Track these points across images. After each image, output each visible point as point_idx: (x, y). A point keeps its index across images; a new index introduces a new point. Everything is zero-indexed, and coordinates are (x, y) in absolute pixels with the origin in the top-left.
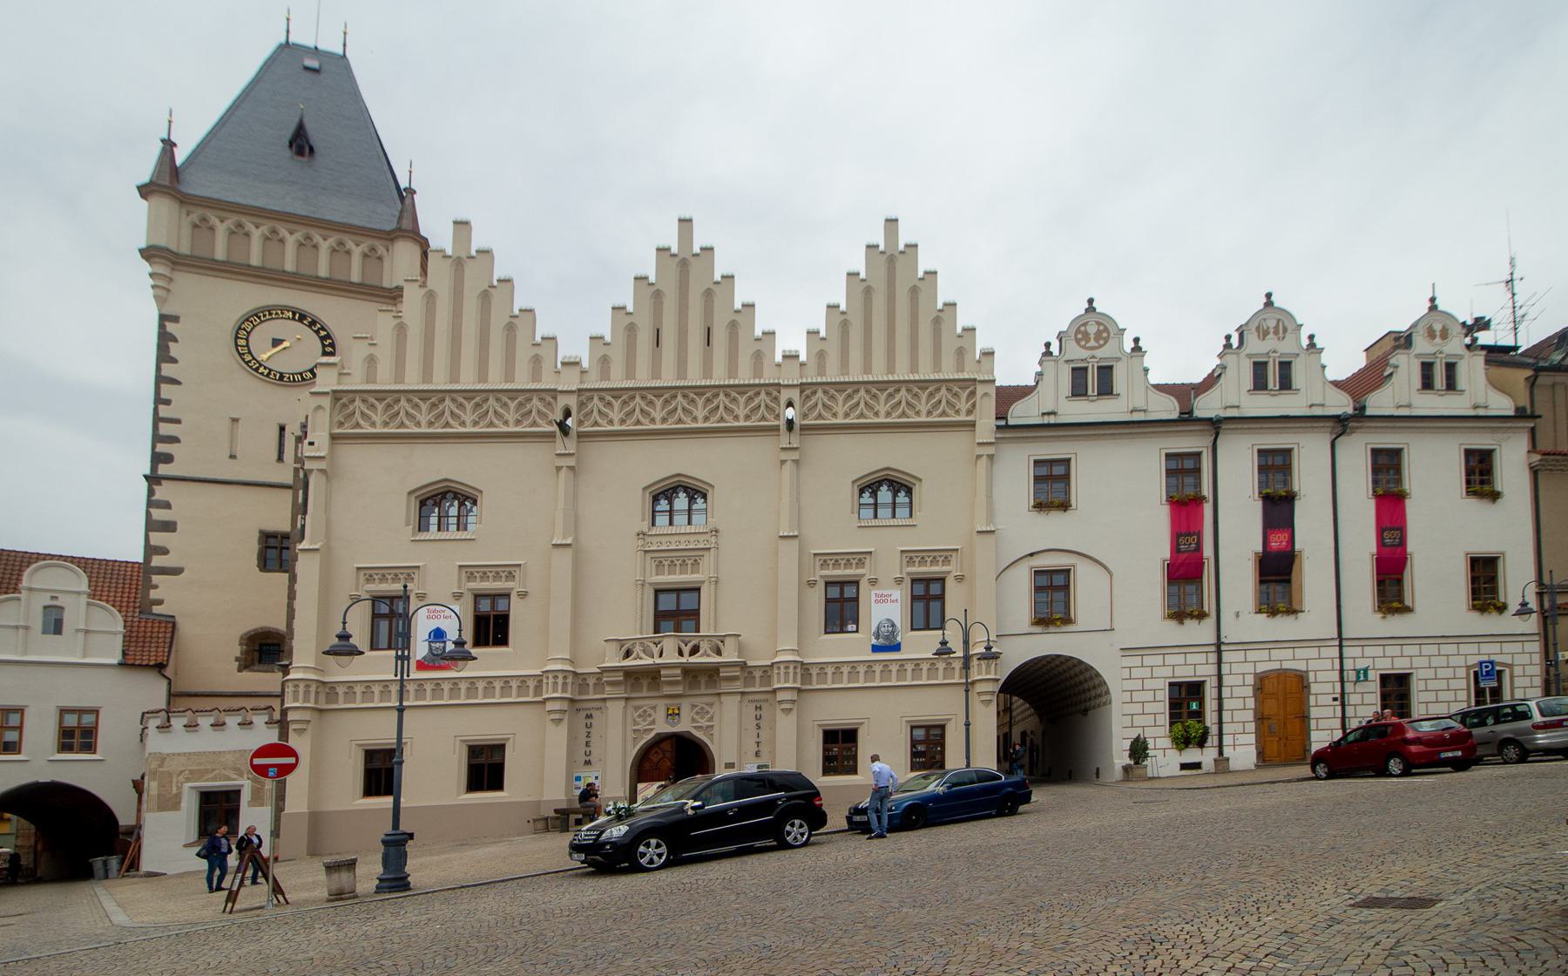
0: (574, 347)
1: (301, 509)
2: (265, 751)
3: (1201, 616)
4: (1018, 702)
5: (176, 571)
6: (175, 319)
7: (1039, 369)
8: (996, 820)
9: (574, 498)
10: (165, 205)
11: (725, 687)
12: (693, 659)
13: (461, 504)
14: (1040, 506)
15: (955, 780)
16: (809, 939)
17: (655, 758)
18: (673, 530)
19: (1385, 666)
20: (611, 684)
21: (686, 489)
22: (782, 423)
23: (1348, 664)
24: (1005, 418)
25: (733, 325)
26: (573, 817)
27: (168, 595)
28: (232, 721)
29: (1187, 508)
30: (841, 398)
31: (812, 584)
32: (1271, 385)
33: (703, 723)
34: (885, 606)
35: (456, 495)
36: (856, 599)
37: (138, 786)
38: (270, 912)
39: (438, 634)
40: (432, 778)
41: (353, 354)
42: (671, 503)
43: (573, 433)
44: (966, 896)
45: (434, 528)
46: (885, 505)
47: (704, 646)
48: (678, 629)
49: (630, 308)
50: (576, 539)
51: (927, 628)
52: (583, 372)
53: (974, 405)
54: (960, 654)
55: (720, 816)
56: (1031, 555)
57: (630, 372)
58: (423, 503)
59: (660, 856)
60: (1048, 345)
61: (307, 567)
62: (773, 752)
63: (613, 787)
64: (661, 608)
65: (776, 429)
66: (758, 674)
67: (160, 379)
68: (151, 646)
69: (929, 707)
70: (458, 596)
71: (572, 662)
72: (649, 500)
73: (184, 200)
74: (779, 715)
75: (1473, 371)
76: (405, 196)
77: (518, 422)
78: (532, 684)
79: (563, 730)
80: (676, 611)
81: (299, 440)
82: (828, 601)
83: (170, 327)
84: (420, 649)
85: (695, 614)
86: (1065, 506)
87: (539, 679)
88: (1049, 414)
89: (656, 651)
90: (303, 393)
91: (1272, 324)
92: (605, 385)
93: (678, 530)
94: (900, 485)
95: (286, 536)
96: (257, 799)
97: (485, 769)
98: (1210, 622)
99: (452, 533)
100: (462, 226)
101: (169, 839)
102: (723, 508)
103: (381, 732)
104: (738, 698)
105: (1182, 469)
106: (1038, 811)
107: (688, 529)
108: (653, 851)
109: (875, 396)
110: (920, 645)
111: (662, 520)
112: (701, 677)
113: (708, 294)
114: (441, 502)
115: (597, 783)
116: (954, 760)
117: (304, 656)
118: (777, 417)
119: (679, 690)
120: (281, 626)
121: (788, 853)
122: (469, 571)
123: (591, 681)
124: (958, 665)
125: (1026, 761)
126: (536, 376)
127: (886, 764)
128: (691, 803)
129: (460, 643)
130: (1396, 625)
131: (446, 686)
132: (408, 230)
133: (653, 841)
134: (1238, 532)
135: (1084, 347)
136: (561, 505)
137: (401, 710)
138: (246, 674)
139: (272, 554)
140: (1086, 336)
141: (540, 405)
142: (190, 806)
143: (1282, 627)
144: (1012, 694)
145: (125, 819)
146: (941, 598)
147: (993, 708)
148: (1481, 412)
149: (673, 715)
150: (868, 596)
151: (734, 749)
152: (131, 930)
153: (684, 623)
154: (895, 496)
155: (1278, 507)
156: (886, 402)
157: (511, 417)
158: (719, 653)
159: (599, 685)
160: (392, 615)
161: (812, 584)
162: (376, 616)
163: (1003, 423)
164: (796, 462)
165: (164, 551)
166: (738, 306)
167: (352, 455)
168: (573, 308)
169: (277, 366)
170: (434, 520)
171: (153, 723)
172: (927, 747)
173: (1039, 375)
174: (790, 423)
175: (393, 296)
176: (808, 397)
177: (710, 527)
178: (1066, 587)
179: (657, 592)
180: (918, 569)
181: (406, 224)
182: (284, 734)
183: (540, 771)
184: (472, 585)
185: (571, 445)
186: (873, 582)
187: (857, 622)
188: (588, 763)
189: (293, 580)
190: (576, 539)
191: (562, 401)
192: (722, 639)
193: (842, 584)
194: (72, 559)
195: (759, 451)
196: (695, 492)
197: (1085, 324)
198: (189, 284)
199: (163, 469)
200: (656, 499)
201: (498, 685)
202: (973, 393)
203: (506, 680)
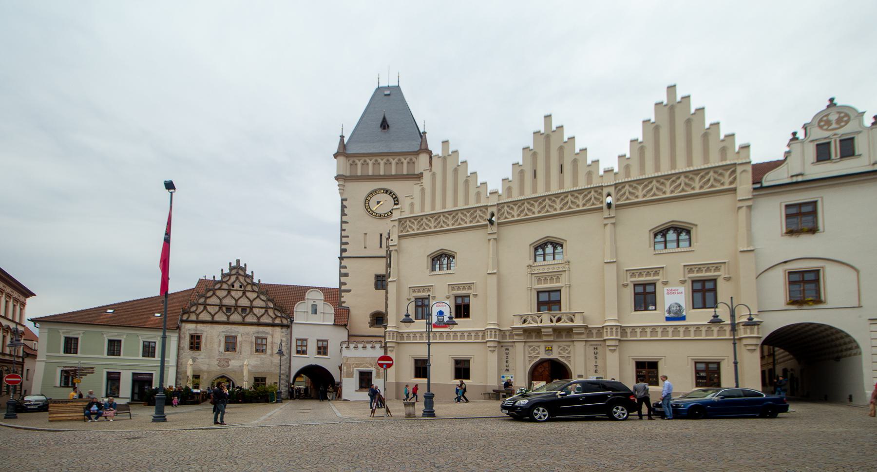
0: (495, 185)
1: (389, 265)
2: (381, 358)
4: (779, 351)
5: (349, 291)
6: (346, 200)
7: (787, 149)
8: (759, 420)
9: (497, 253)
10: (342, 159)
11: (576, 338)
12: (558, 324)
13: (448, 259)
14: (791, 232)
15: (727, 394)
16: (626, 465)
17: (540, 370)
18: (545, 263)
20: (517, 335)
21: (552, 243)
22: (604, 205)
24: (760, 182)
25: (575, 161)
26: (501, 394)
27: (348, 300)
28: (369, 346)
30: (468, 215)
31: (625, 286)
32: (833, 156)
33: (565, 354)
34: (674, 295)
35: (446, 255)
36: (654, 293)
37: (340, 368)
38: (386, 418)
39: (441, 313)
40: (442, 374)
41: (405, 203)
42: (544, 251)
43: (496, 224)
44: (730, 458)
45: (437, 269)
46: (672, 241)
47: (564, 318)
48: (550, 309)
49: (521, 163)
50: (498, 270)
51: (704, 307)
52: (499, 196)
53: (735, 179)
54: (728, 322)
55: (575, 400)
56: (785, 262)
57: (522, 192)
58: (433, 260)
59: (545, 416)
60: (794, 134)
61: (392, 287)
62: (605, 371)
63: (520, 382)
64: (541, 300)
65: (601, 208)
66: (594, 332)
67: (342, 222)
68: (342, 318)
69: (708, 352)
70: (448, 297)
71: (498, 325)
72: (532, 250)
73: (347, 156)
74: (608, 353)
76: (422, 136)
77: (471, 222)
78: (481, 334)
79: (495, 354)
80: (548, 301)
81: (387, 239)
82: (636, 294)
83: (345, 203)
84: (434, 320)
85: (558, 302)
86: (813, 230)
87: (484, 332)
88: (797, 175)
89: (539, 320)
90: (388, 221)
92: (510, 200)
93: (549, 262)
94: (682, 230)
95: (384, 276)
96: (378, 376)
97: (462, 370)
99: (445, 271)
100: (445, 143)
101: (350, 386)
102: (571, 250)
103: (421, 352)
104: (584, 343)
106: (795, 418)
107: (554, 262)
108: (540, 413)
109: (577, 197)
110: (703, 316)
111: (540, 259)
112: (563, 333)
113: (561, 149)
114: (441, 258)
115: (512, 380)
116: (727, 382)
117: (392, 322)
118: (602, 202)
119: (551, 338)
120: (384, 311)
121: (615, 423)
122: (452, 287)
123: (508, 333)
124: (728, 329)
125: (788, 386)
126: (478, 201)
127: (678, 382)
128: (559, 392)
129: (450, 318)
131: (445, 335)
132: (424, 149)
133: (541, 409)
135: (826, 130)
136: (491, 256)
137: (429, 344)
138: (372, 328)
139: (379, 283)
140: (828, 123)
141: (528, 206)
142: (356, 376)
144: (775, 345)
145: (337, 380)
146: (714, 290)
147: (757, 355)
149: (549, 350)
151: (582, 366)
152: (344, 419)
153: (553, 307)
154: (678, 235)
156: (671, 185)
157: (468, 220)
158: (572, 321)
159: (511, 335)
160: (423, 306)
161: (625, 286)
162: (417, 306)
163: (758, 186)
164: (614, 224)
165: (345, 284)
166: (577, 151)
167: (407, 243)
168: (493, 169)
169: (378, 212)
170: (437, 266)
171: (344, 346)
172: (707, 374)
173: (788, 154)
174: (609, 205)
175: (419, 176)
176: (620, 190)
177: (565, 260)
178: (817, 281)
179: (538, 293)
180: (696, 275)
181: (423, 147)
182: (386, 352)
183: (486, 373)
184: (415, 294)
185: (494, 229)
186: (665, 283)
187: (655, 305)
188: (507, 370)
189: (387, 293)
190: (498, 270)
191: (490, 210)
192: (574, 314)
193: (644, 285)
194: (318, 288)
195: (592, 221)
196: (556, 244)
197: (827, 115)
198: (351, 186)
199: (344, 255)
200: (536, 249)
201: (466, 334)
202: (734, 172)
203: (470, 332)
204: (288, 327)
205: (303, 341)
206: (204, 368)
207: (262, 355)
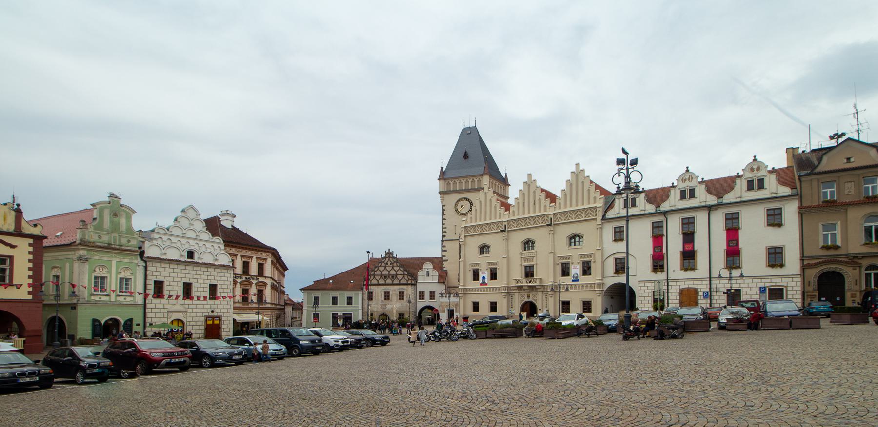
3: (662, 271)
14: (615, 240)
23: (713, 286)
29: (658, 239)
34: (576, 269)
39: (484, 278)
80: (529, 273)
91: (687, 177)
93: (529, 253)
98: (665, 273)
134: (674, 245)
143: (690, 274)
148: (774, 195)
149: (529, 297)
150: (571, 267)
155: (689, 236)
179: (526, 267)
204: (415, 285)
206: (375, 309)
207: (402, 301)
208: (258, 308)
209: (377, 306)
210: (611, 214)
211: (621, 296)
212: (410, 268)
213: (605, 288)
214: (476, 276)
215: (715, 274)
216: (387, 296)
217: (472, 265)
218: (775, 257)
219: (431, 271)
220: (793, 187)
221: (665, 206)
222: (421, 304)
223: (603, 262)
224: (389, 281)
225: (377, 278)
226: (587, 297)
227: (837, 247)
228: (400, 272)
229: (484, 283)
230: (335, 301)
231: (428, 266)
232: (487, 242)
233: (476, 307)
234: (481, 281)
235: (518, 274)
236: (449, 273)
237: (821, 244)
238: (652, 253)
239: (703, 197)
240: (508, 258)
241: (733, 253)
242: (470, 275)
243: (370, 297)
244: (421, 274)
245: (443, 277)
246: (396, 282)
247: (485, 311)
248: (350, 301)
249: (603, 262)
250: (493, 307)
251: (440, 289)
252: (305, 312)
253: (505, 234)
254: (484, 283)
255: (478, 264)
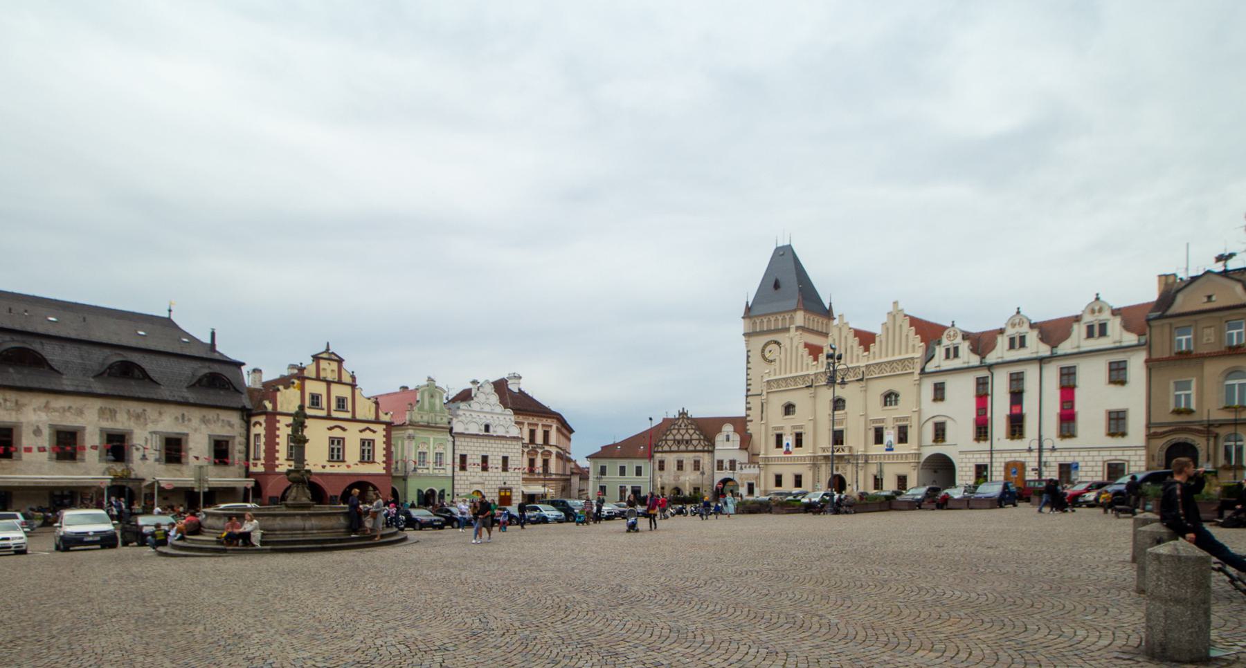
9: (815, 405)
19: (1062, 460)
29: (982, 398)
34: (890, 436)
75: (1115, 326)
80: (838, 438)
105: (982, 384)
130: (1068, 443)
150: (885, 432)
155: (1017, 396)
204: (712, 452)
205: (720, 463)
208: (545, 480)
209: (668, 478)
210: (930, 367)
211: (942, 468)
212: (707, 429)
213: (922, 460)
214: (779, 444)
215: (1047, 445)
216: (680, 466)
217: (775, 428)
218: (1117, 423)
219: (731, 435)
220: (1140, 334)
221: (991, 358)
222: (719, 476)
223: (920, 428)
224: (683, 447)
225: (670, 443)
226: (902, 470)
227: (1189, 412)
228: (695, 436)
229: (787, 452)
230: (622, 471)
231: (728, 429)
232: (793, 401)
233: (779, 481)
234: (784, 448)
235: (826, 440)
236: (754, 437)
237: (1172, 407)
238: (974, 416)
239: (1035, 347)
240: (815, 421)
241: (1067, 419)
242: (773, 441)
243: (662, 468)
244: (720, 439)
245: (746, 442)
246: (691, 448)
247: (788, 486)
248: (639, 472)
249: (920, 428)
250: (798, 481)
251: (742, 457)
252: (591, 483)
253: (812, 390)
254: (787, 452)
255: (782, 428)
